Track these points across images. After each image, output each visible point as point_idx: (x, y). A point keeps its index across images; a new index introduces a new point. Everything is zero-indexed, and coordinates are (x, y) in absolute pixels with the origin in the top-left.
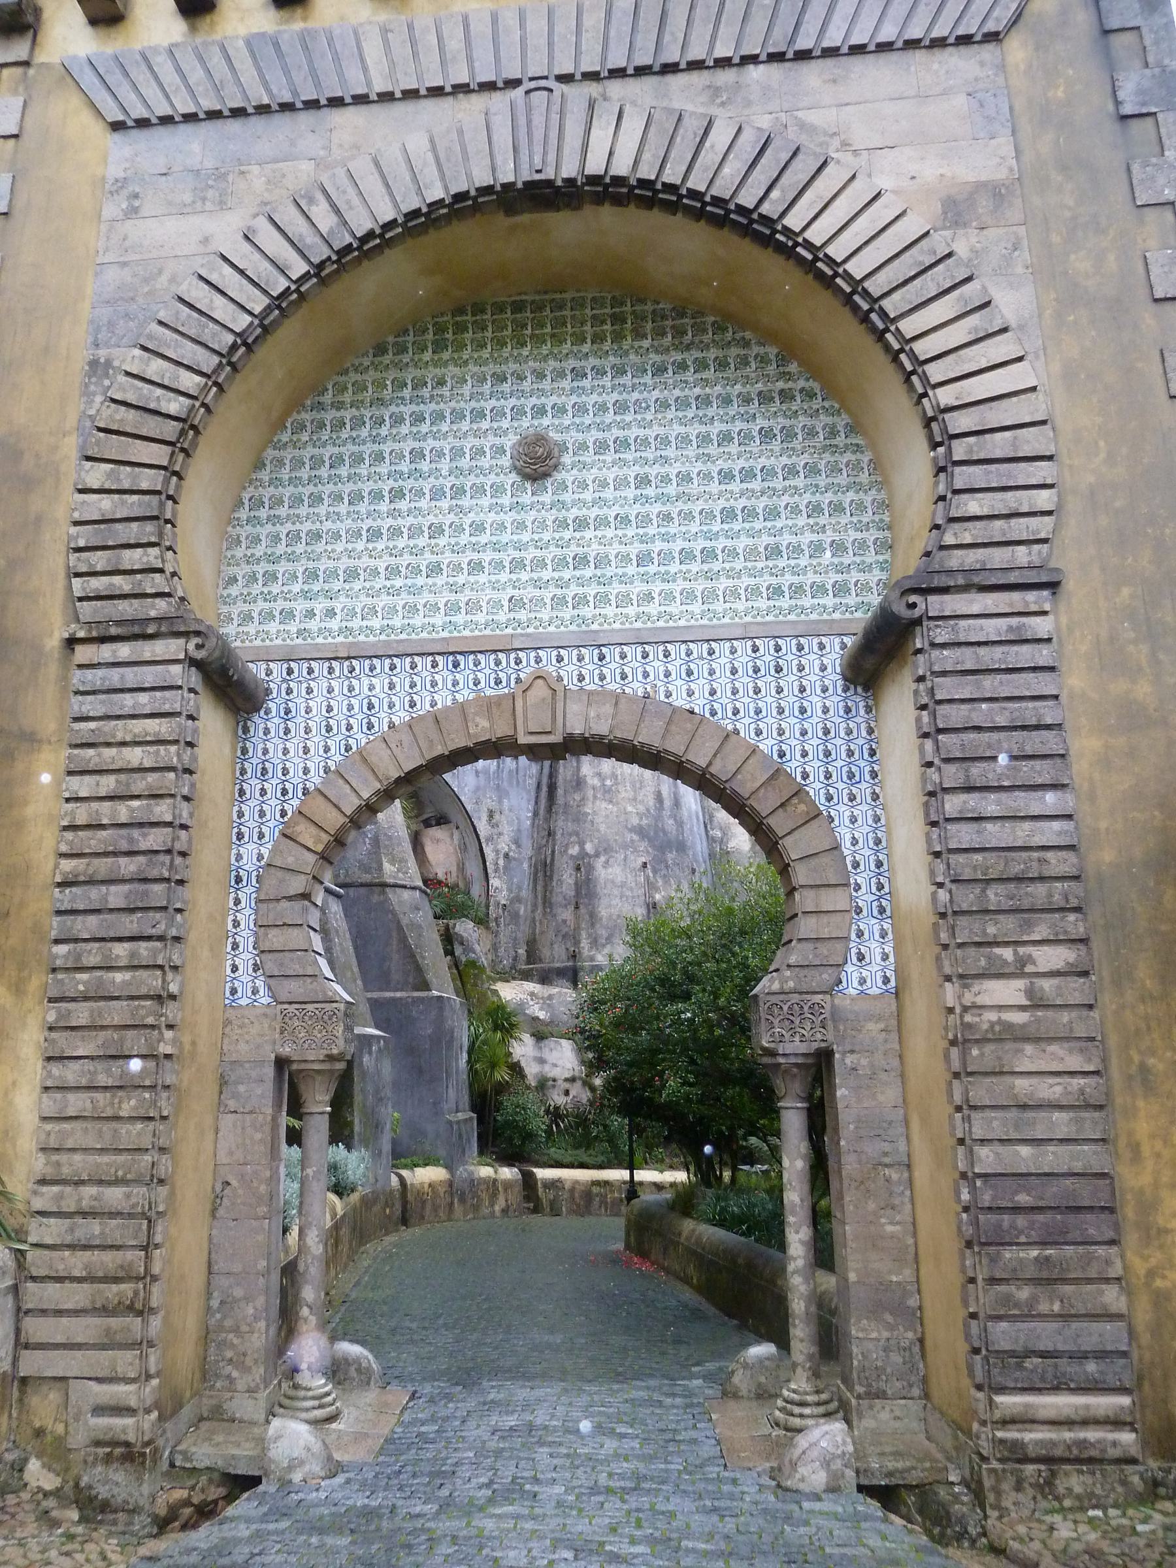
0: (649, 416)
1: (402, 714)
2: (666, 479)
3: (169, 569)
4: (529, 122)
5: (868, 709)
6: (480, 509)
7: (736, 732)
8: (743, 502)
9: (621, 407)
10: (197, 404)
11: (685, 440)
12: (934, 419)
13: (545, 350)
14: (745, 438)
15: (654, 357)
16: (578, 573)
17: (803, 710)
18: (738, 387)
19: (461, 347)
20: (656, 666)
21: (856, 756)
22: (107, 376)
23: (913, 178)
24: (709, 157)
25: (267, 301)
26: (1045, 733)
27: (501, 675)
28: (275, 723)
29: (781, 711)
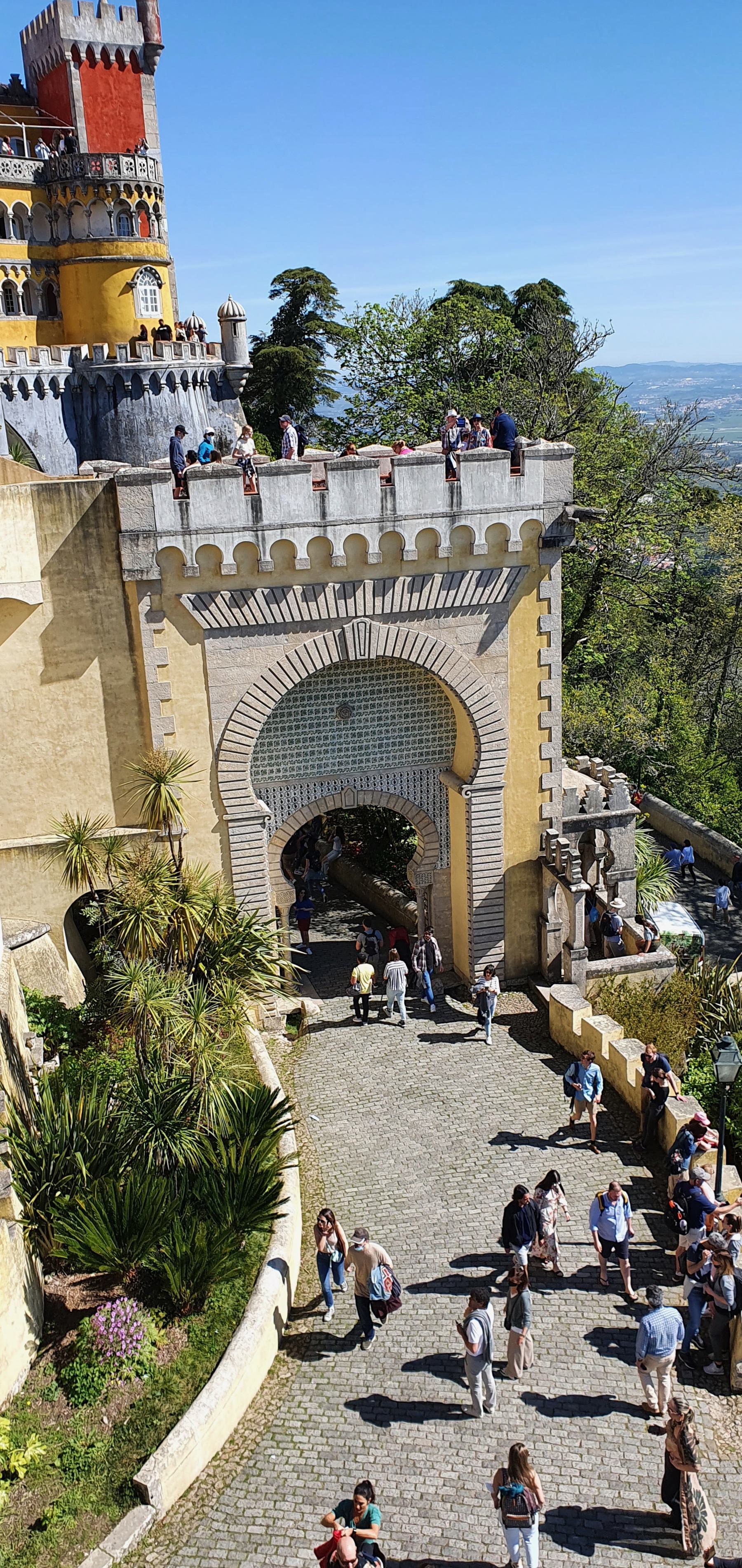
2: (387, 718)
9: (372, 692)
11: (394, 704)
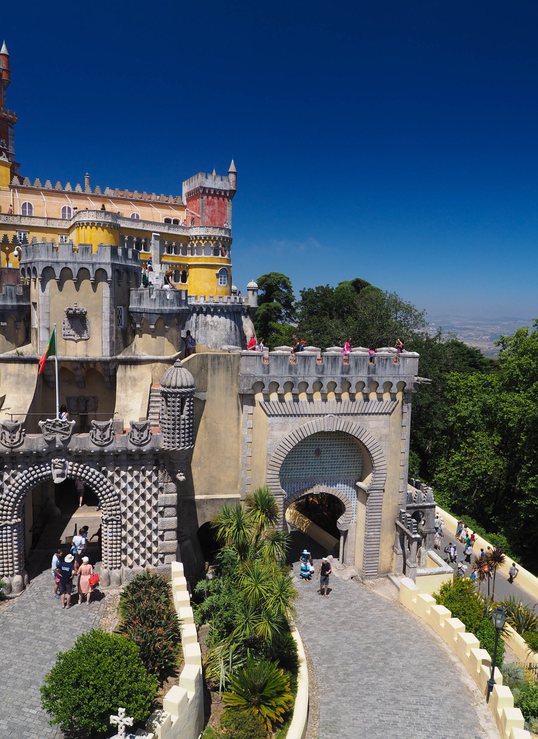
9: (330, 445)
11: (338, 450)
24: (352, 429)
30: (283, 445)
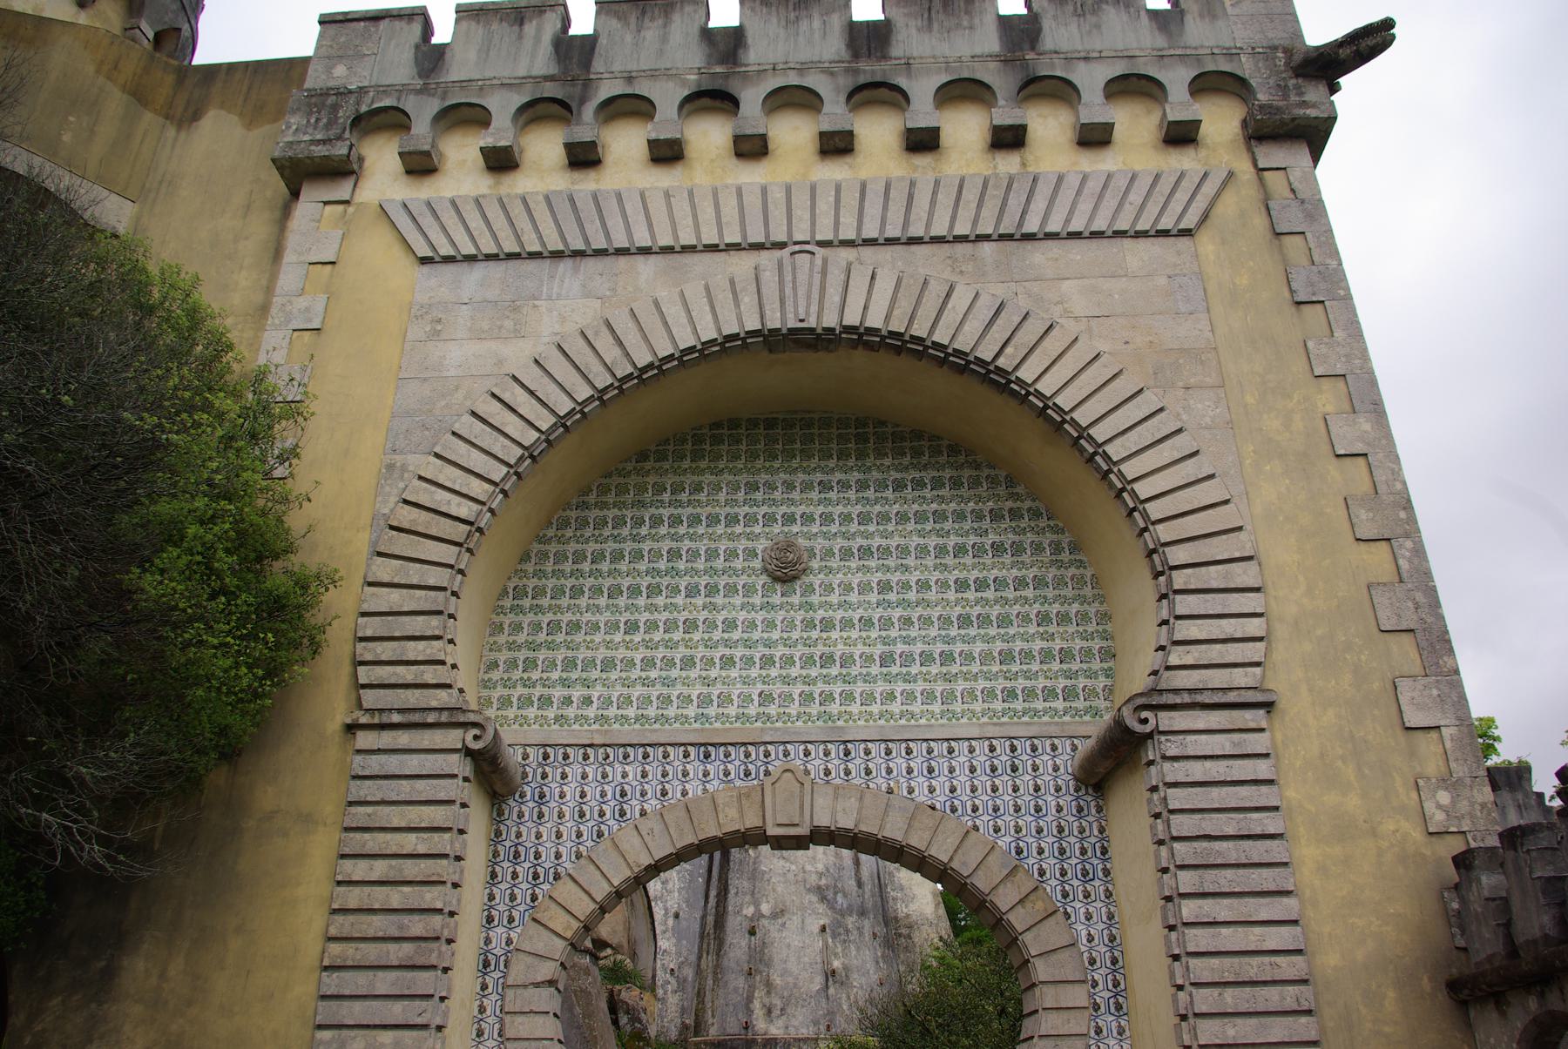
0: (890, 527)
1: (654, 802)
3: (450, 661)
4: (794, 282)
5: (1099, 810)
6: (733, 607)
7: (976, 828)
8: (977, 610)
9: (864, 519)
10: (485, 509)
12: (1154, 551)
13: (795, 463)
14: (979, 551)
15: (895, 475)
16: (824, 671)
17: (1038, 809)
18: (971, 504)
19: (718, 457)
20: (899, 764)
21: (1089, 854)
22: (402, 478)
23: (1127, 343)
25: (554, 420)
26: (1268, 842)
27: (750, 766)
28: (529, 807)
29: (1017, 809)
30: (492, 410)
